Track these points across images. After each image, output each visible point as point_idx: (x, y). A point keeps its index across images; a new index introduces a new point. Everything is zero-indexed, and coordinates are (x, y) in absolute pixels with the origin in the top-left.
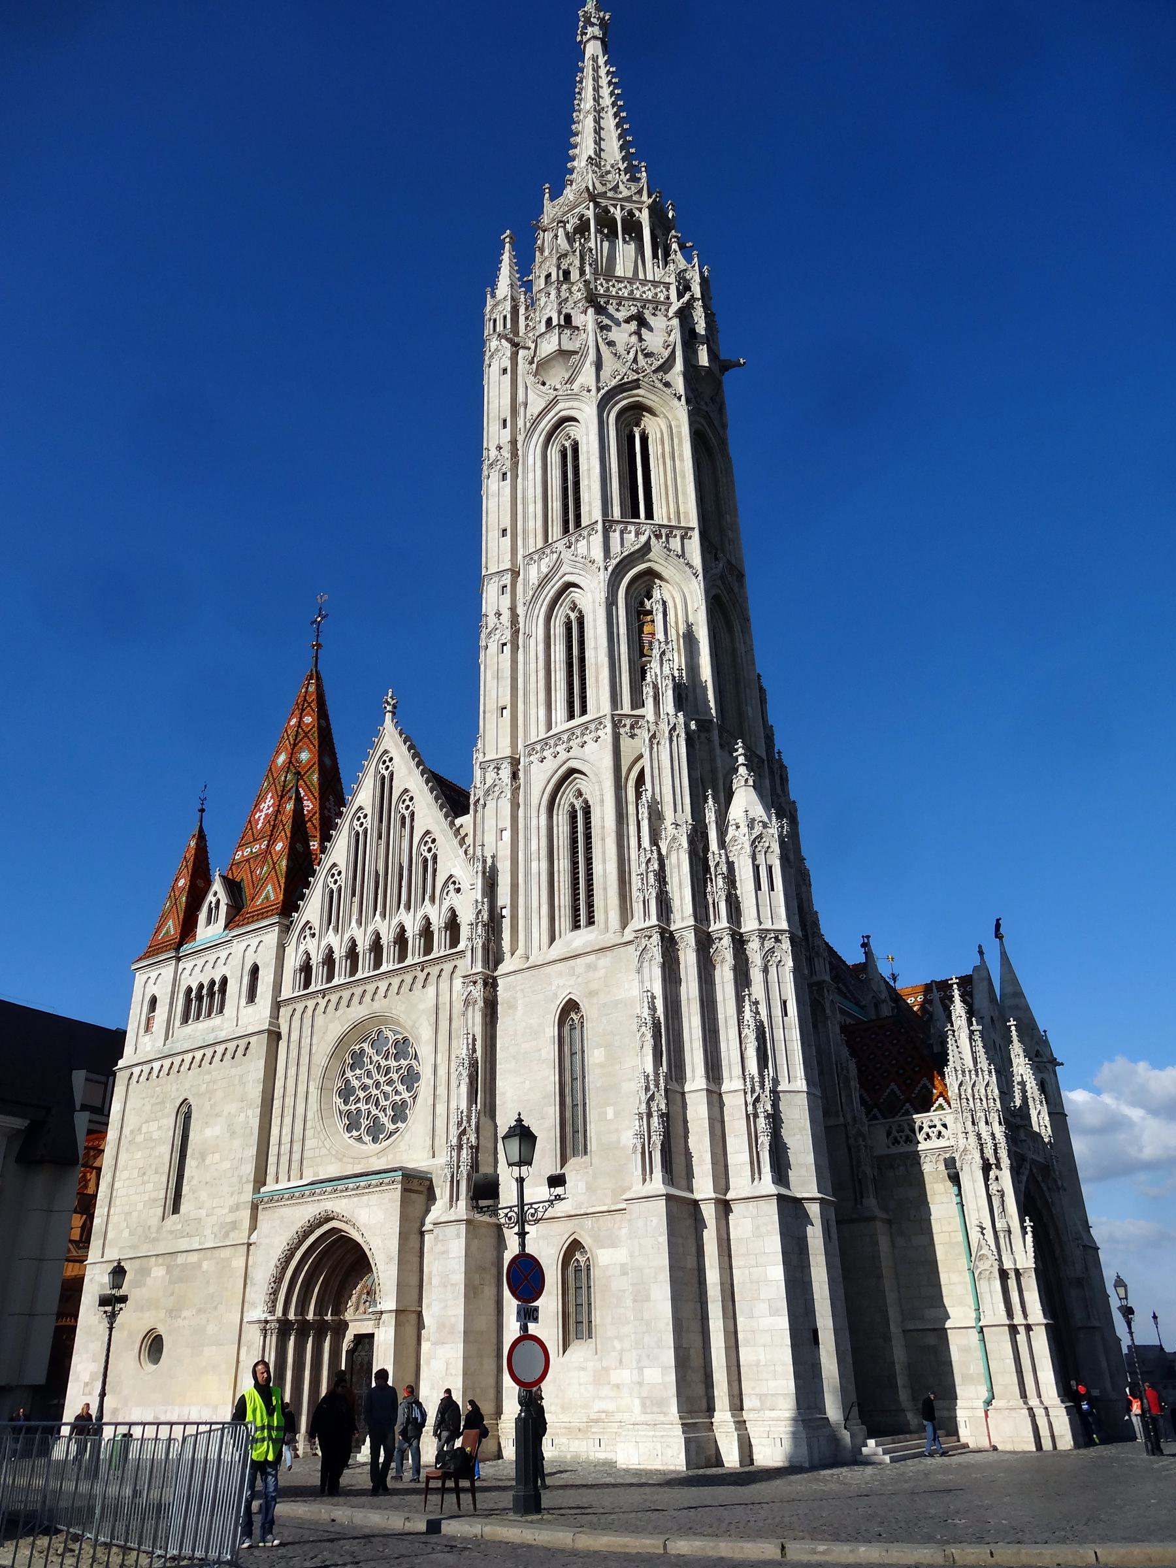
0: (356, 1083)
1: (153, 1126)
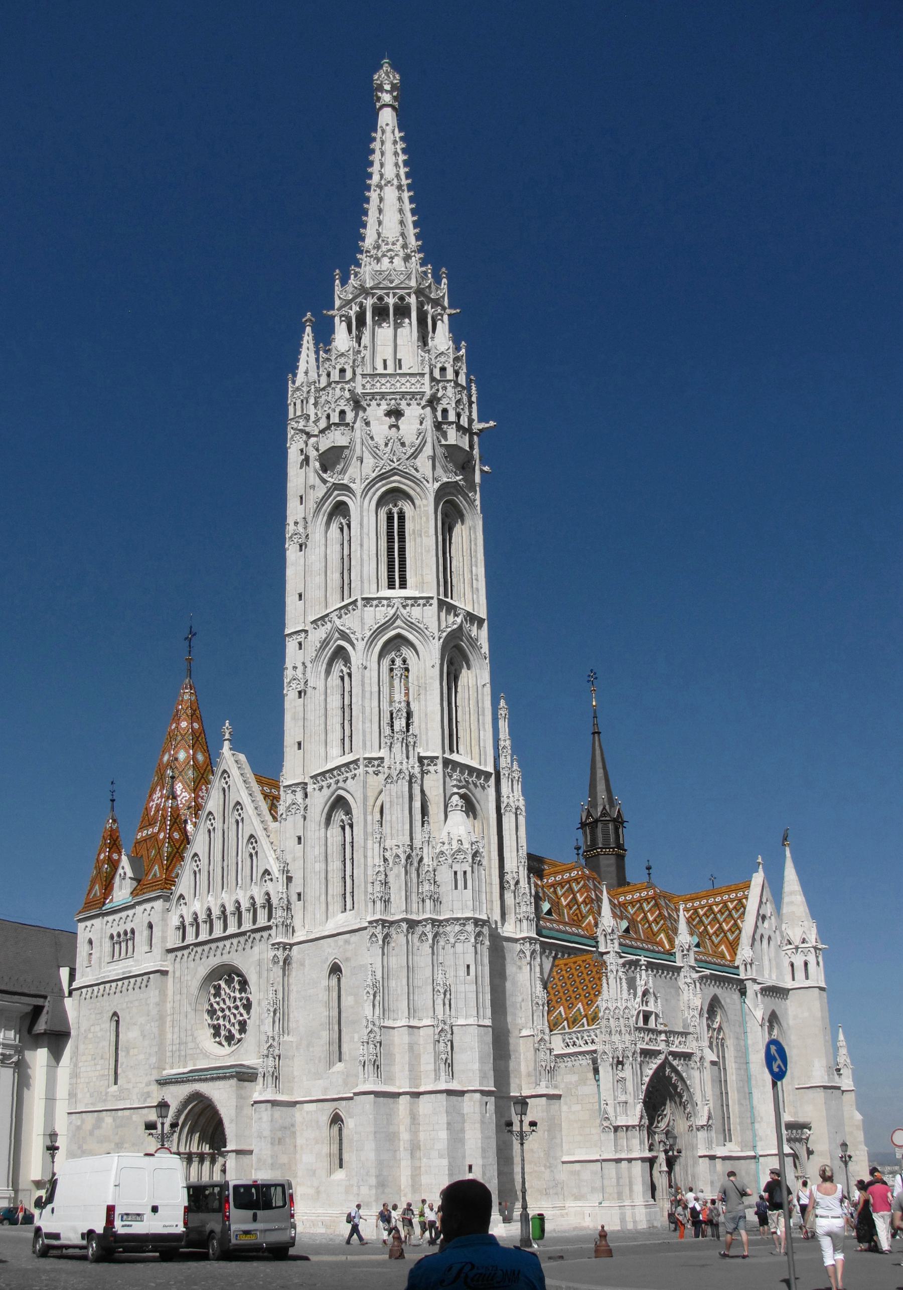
0: (215, 1006)
1: (97, 1028)
